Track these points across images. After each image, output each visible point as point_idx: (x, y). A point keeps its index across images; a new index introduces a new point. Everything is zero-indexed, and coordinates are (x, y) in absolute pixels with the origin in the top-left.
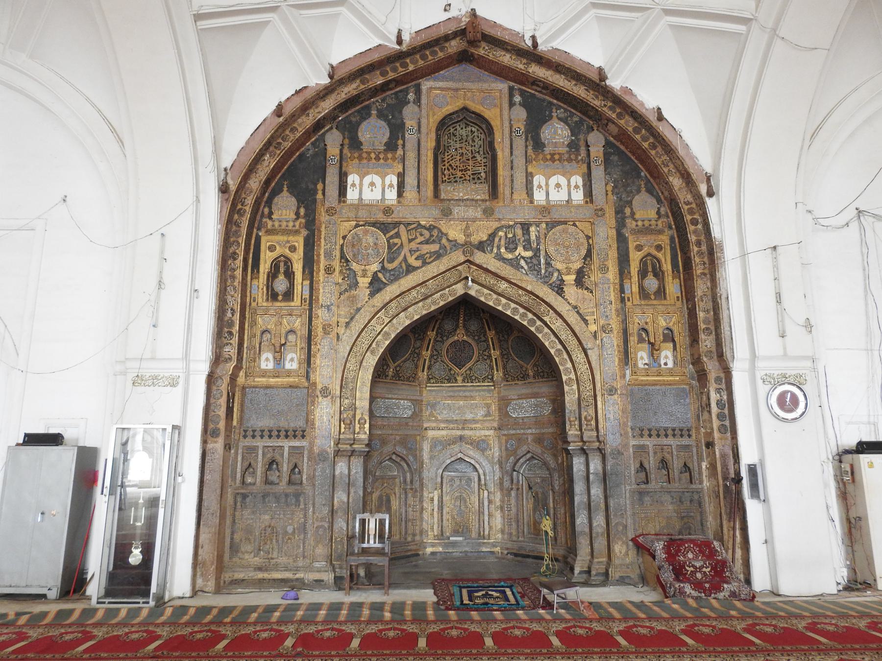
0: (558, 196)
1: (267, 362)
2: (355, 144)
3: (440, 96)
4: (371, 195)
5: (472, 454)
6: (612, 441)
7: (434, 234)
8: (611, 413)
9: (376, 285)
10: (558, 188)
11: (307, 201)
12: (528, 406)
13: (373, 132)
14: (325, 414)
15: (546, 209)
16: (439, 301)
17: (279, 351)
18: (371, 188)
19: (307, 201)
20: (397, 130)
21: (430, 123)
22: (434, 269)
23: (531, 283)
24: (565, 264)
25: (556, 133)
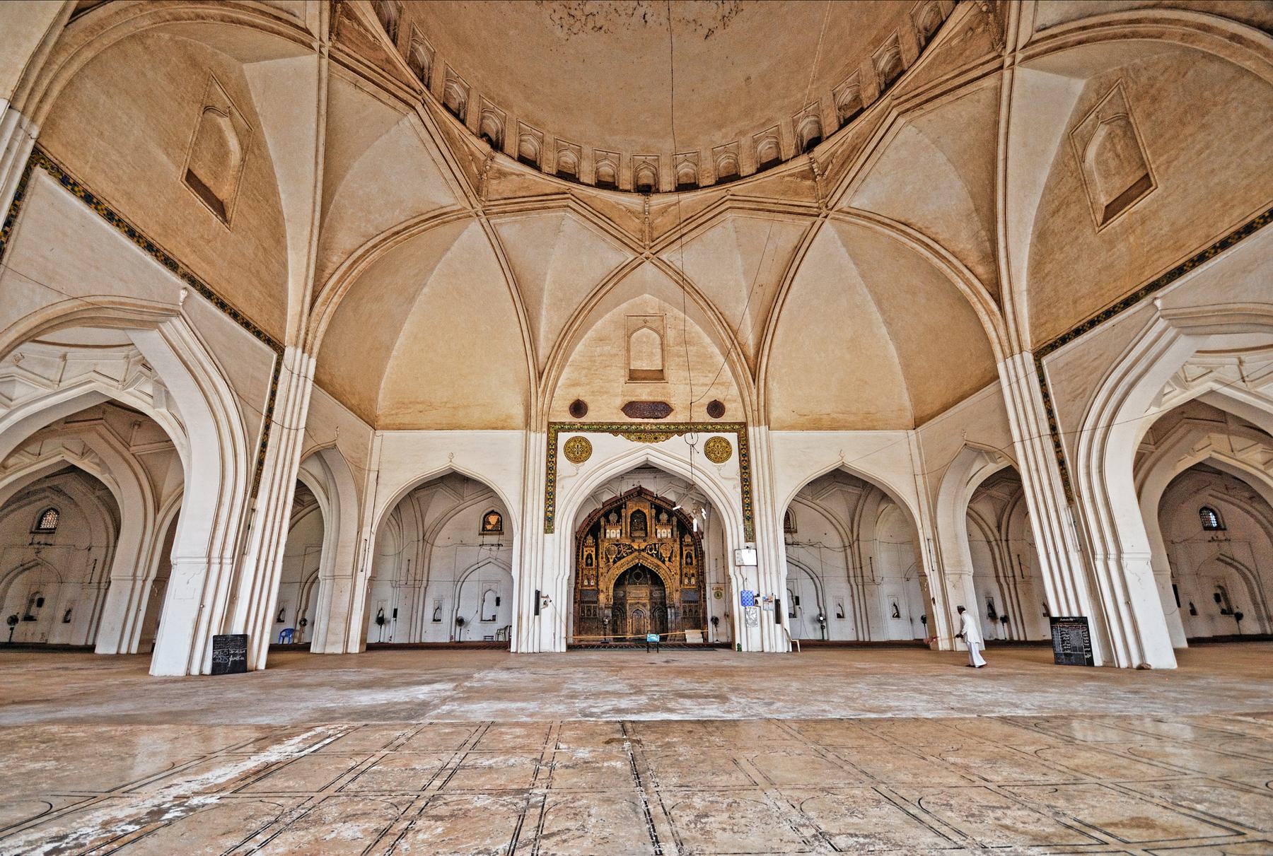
0: (664, 535)
1: (586, 583)
2: (608, 521)
3: (632, 507)
4: (613, 536)
5: (641, 608)
6: (677, 605)
7: (630, 547)
8: (676, 596)
9: (615, 562)
10: (664, 533)
11: (596, 538)
12: (657, 594)
13: (613, 517)
14: (602, 597)
15: (660, 540)
16: (631, 565)
17: (589, 580)
18: (613, 533)
19: (596, 538)
20: (620, 516)
21: (630, 513)
22: (630, 557)
23: (656, 561)
24: (666, 555)
25: (664, 517)
